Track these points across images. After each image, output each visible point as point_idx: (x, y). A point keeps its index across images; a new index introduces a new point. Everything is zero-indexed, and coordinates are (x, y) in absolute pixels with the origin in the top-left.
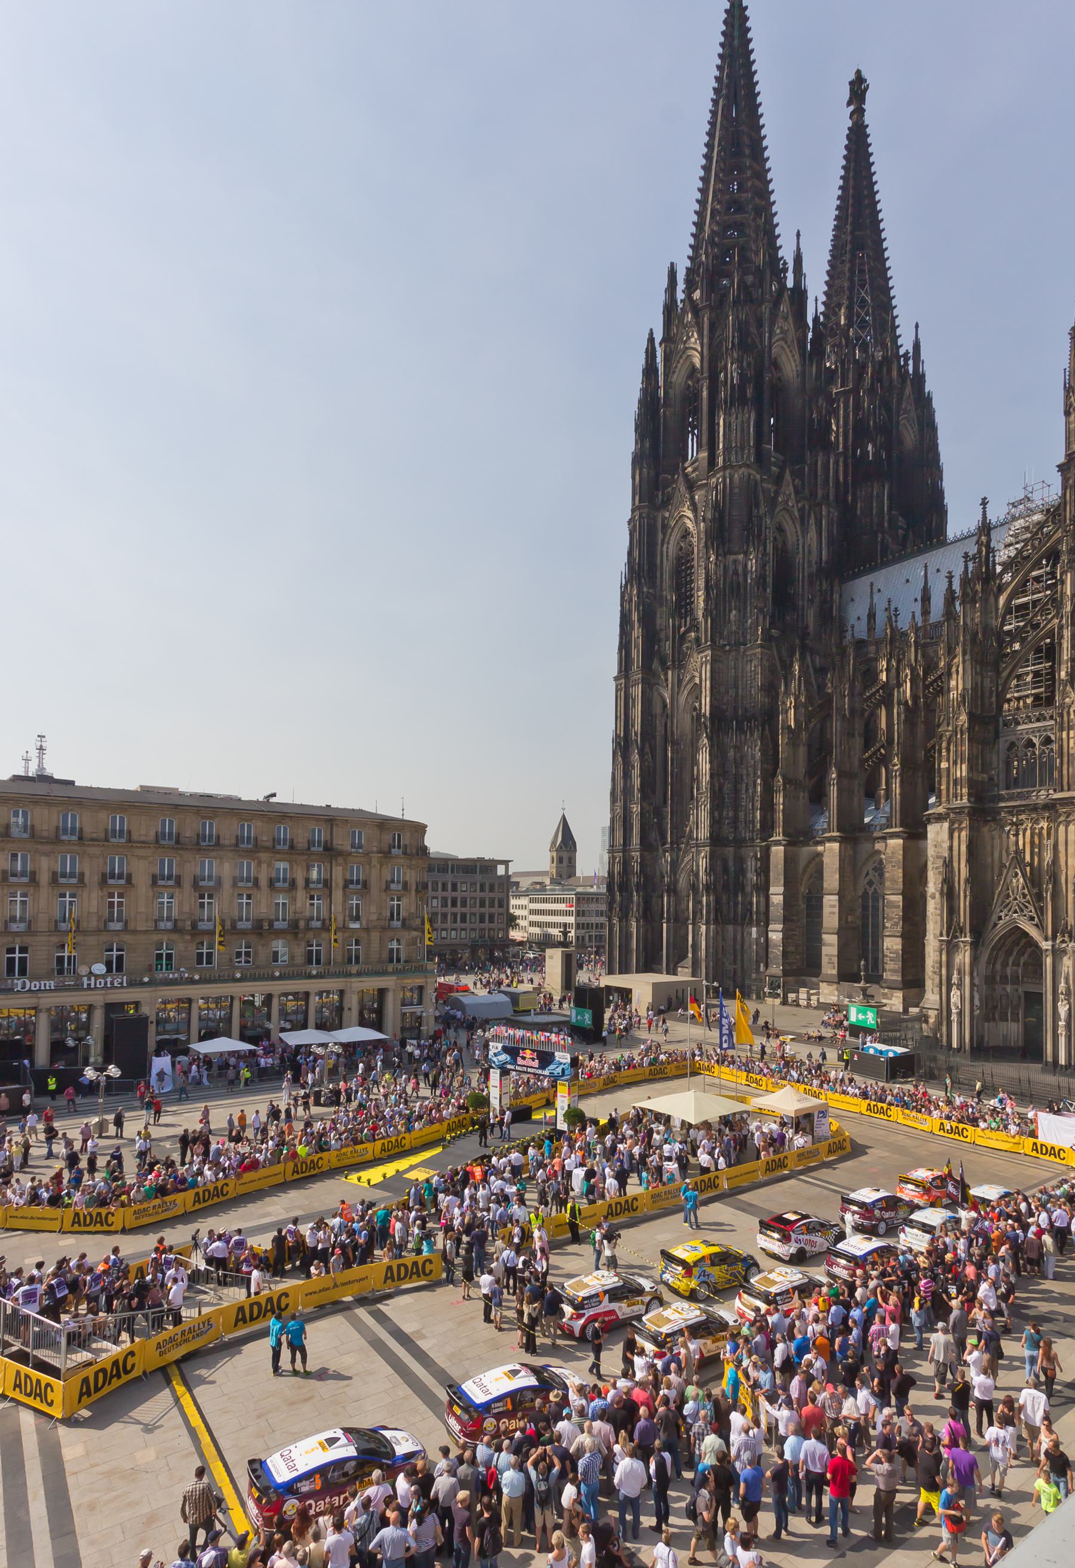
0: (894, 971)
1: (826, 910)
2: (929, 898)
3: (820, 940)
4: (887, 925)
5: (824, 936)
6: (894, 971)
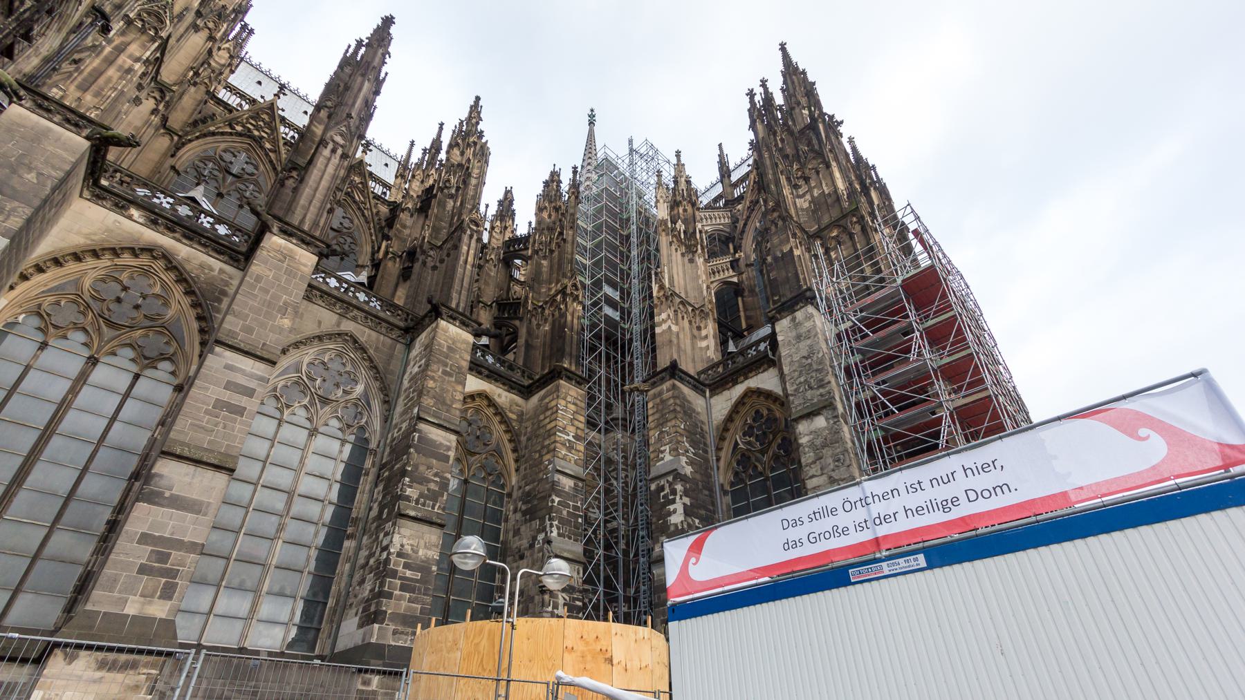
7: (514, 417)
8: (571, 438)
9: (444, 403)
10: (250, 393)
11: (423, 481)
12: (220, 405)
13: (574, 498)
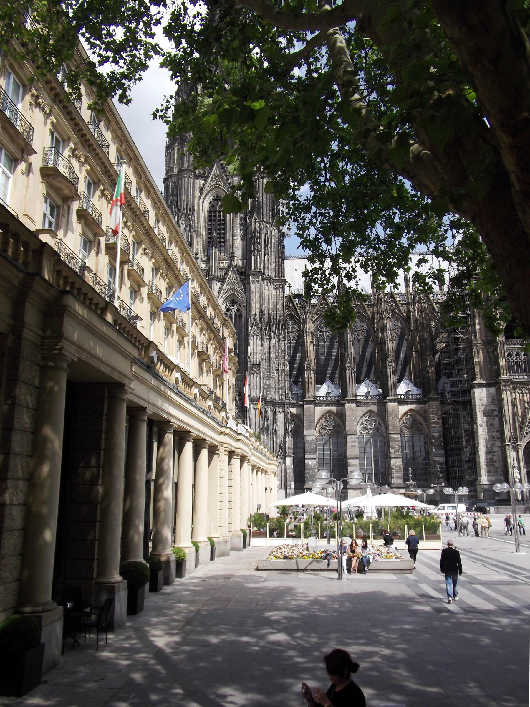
0: (398, 477)
1: (349, 444)
2: (479, 426)
3: (348, 462)
4: (392, 451)
5: (349, 460)
6: (398, 477)
7: (422, 412)
8: (436, 420)
9: (395, 426)
10: (355, 442)
11: (394, 448)
12: (352, 446)
13: (439, 438)
